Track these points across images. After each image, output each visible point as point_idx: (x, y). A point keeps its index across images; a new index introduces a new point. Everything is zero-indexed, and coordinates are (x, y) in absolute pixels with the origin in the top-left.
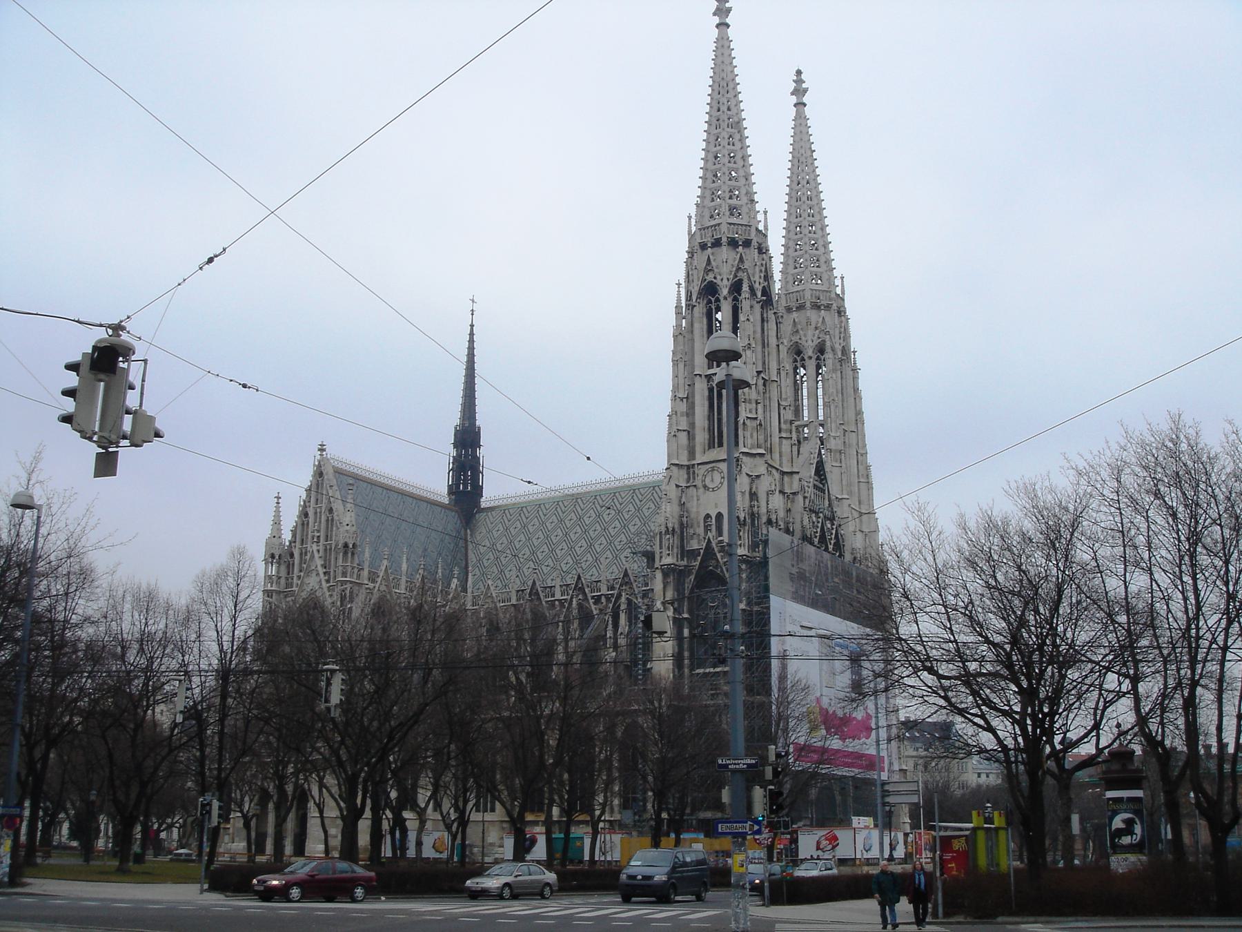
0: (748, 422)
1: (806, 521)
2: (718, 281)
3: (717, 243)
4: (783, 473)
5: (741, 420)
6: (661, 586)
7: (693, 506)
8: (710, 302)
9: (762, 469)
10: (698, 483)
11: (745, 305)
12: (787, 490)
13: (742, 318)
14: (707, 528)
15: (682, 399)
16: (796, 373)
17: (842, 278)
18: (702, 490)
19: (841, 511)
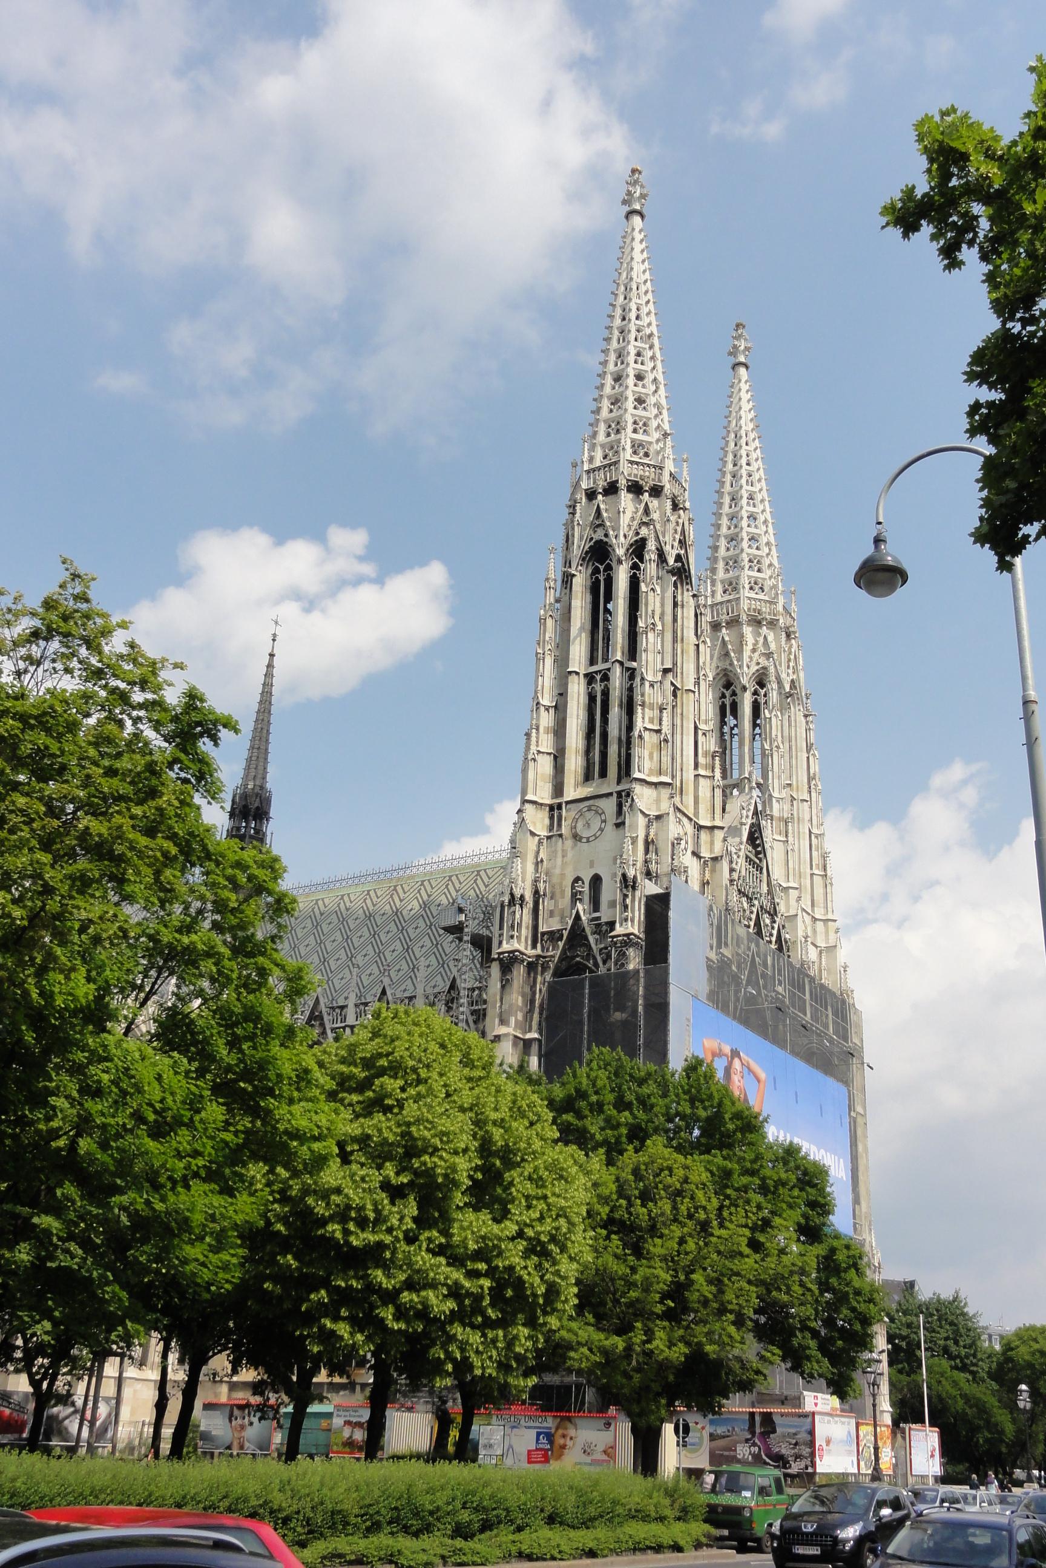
0: (646, 735)
4: (700, 828)
5: (636, 733)
6: (499, 985)
8: (596, 571)
9: (665, 806)
10: (564, 830)
11: (650, 568)
12: (705, 853)
13: (643, 587)
14: (575, 898)
15: (547, 709)
16: (723, 723)
18: (569, 843)
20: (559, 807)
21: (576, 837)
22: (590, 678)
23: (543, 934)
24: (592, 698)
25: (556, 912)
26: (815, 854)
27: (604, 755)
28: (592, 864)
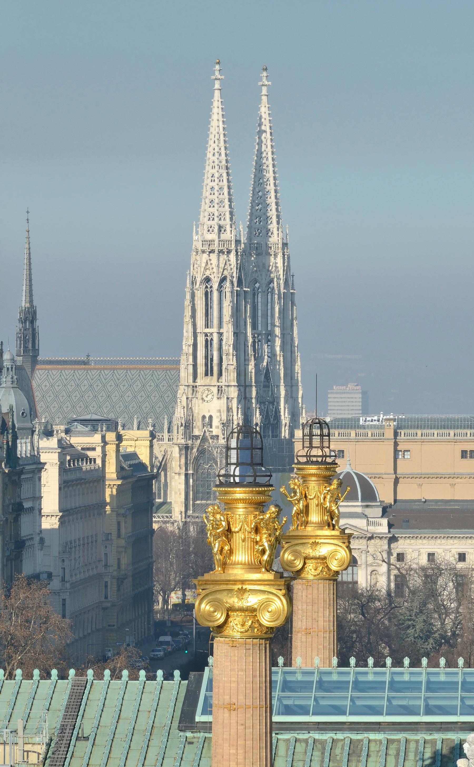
2: (212, 277)
3: (212, 251)
6: (178, 455)
7: (196, 410)
10: (199, 395)
18: (201, 401)
20: (196, 387)
22: (206, 335)
23: (193, 436)
24: (207, 341)
25: (197, 427)
27: (212, 367)
28: (209, 411)
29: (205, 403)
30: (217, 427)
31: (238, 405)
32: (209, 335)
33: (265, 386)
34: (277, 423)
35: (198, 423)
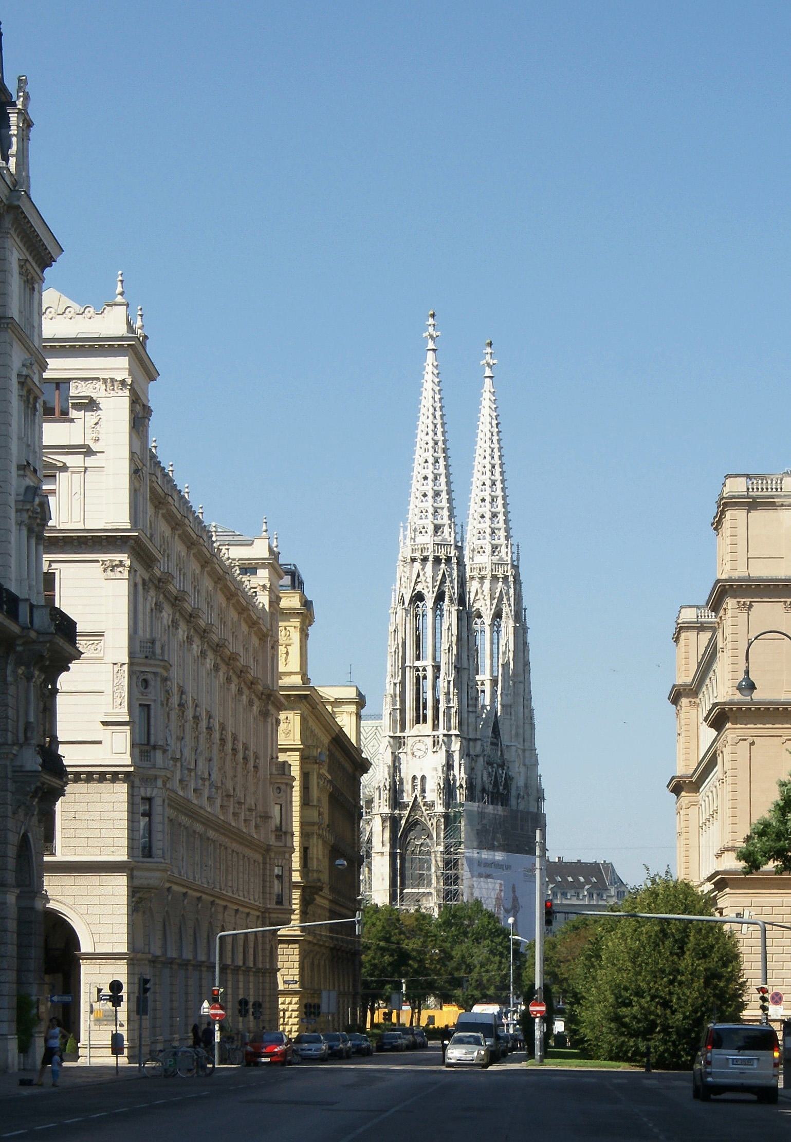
1: (485, 778)
2: (425, 592)
3: (425, 560)
4: (470, 740)
12: (472, 753)
17: (518, 546)
19: (510, 755)
21: (413, 754)
24: (418, 678)
26: (526, 710)
29: (417, 759)
30: (433, 791)
31: (460, 760)
32: (421, 669)
33: (492, 744)
34: (507, 794)
35: (408, 787)
